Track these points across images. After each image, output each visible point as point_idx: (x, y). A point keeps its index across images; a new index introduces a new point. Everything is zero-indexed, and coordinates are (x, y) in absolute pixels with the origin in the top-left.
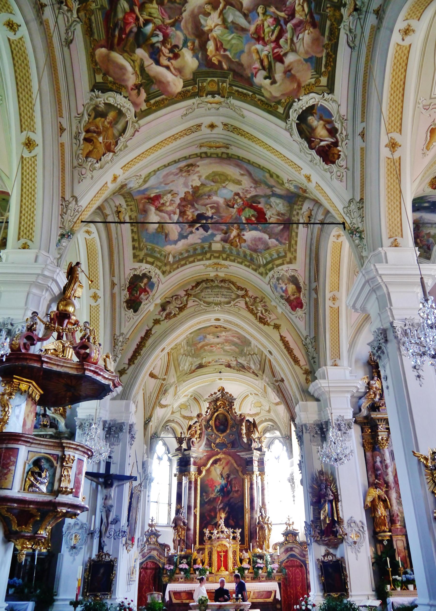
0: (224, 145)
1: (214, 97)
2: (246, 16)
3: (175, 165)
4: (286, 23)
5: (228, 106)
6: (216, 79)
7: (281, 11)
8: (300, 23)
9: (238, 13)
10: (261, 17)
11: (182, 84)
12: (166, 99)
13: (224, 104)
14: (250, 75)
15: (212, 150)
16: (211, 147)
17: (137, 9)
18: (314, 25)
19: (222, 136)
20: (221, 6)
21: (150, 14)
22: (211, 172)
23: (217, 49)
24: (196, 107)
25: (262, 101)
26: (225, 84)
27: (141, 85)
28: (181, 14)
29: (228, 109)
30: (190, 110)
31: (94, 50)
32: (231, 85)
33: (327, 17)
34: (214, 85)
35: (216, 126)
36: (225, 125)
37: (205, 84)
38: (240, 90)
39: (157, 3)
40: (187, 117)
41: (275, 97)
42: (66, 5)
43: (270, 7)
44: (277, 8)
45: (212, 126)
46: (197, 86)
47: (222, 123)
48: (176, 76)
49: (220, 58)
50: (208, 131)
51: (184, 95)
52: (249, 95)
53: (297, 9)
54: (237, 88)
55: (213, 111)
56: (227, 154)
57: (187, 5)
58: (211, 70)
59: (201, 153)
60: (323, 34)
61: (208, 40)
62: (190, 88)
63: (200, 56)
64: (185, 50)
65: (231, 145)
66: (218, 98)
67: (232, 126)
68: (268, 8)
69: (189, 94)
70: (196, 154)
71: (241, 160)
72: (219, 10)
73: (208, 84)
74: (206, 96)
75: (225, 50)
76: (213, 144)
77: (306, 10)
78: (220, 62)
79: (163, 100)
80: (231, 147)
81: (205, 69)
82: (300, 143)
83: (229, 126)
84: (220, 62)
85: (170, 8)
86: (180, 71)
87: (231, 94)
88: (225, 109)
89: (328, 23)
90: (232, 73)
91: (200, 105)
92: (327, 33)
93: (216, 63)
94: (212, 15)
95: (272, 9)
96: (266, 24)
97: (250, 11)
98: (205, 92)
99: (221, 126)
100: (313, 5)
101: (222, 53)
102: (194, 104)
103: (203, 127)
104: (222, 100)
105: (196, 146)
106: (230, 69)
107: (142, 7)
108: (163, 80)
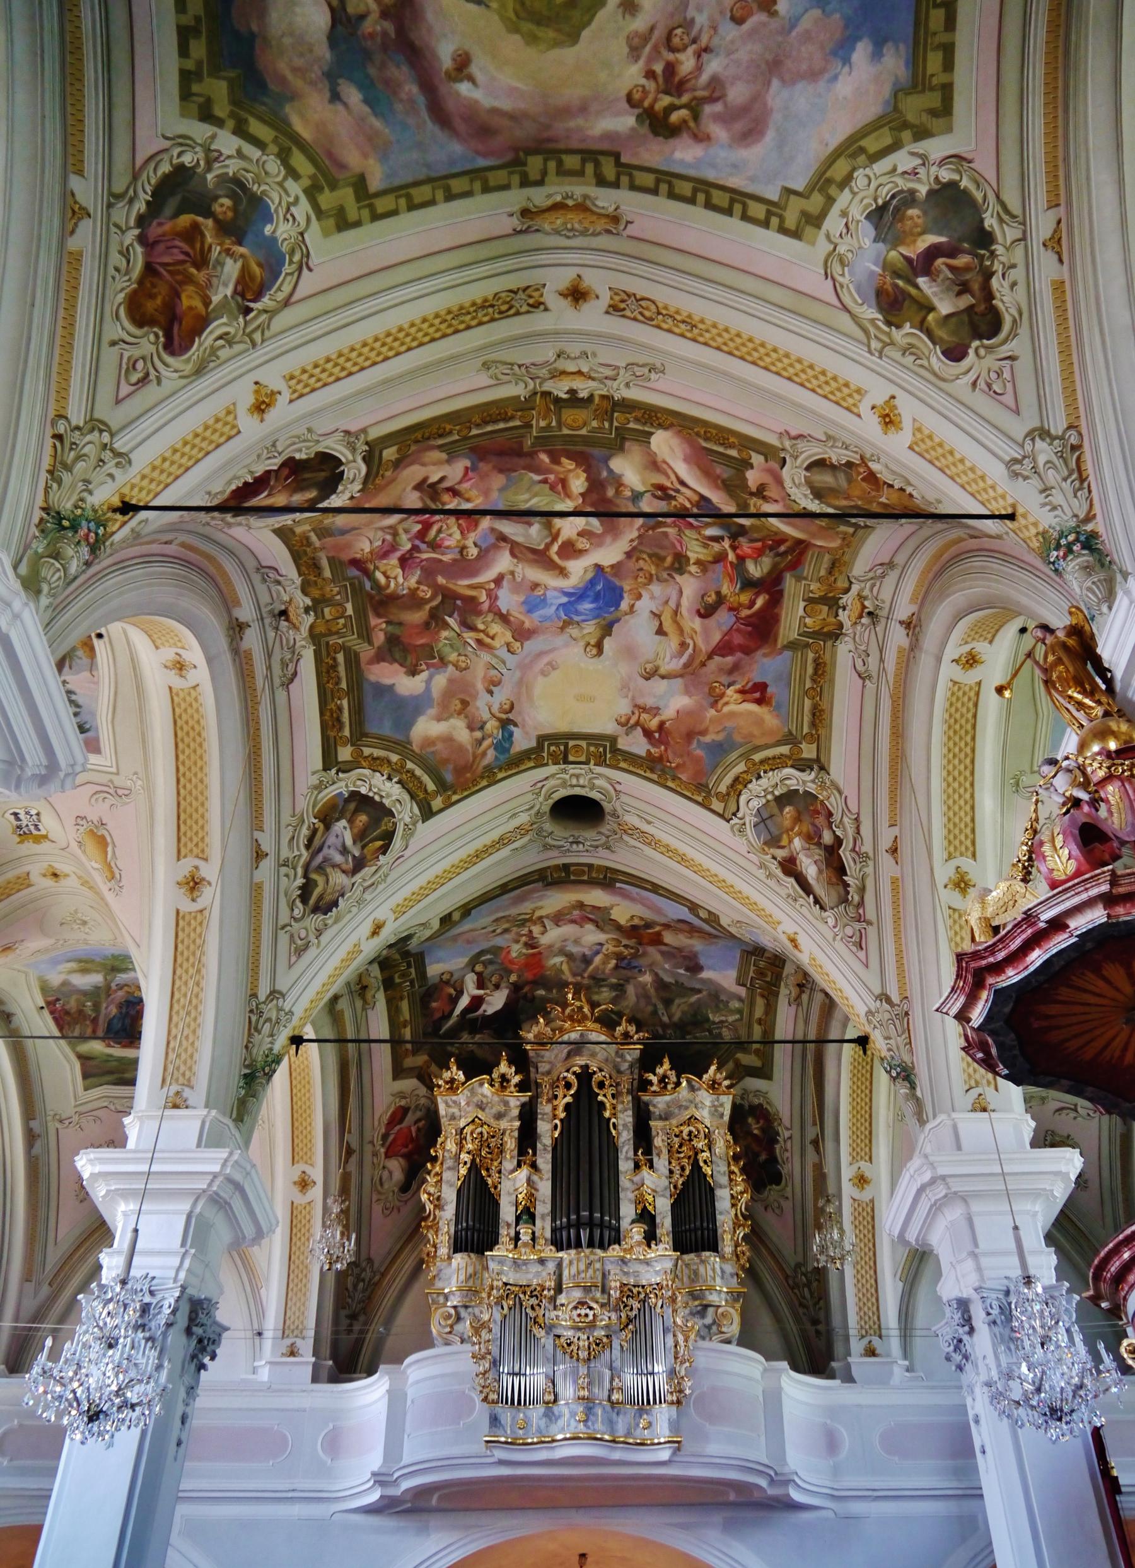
0: (537, 223)
1: (572, 392)
2: (503, 538)
3: (711, 175)
4: (415, 548)
5: (533, 370)
6: (566, 431)
7: (427, 560)
8: (385, 555)
9: (520, 539)
10: (469, 543)
11: (654, 440)
12: (698, 434)
13: (543, 373)
14: (481, 465)
15: (579, 190)
16: (582, 207)
17: (731, 556)
18: (356, 563)
19: (544, 258)
20: (555, 548)
21: (706, 546)
22: (585, 34)
23: (564, 482)
24: (622, 372)
25: (441, 436)
26: (543, 424)
27: (752, 494)
28: (640, 537)
29: (527, 361)
30: (639, 371)
31: (841, 547)
32: (528, 425)
33: (333, 581)
34: (569, 421)
35: (564, 295)
36: (537, 305)
37: (595, 424)
38: (502, 425)
39: (688, 559)
40: (650, 360)
41: (411, 464)
42: (864, 607)
43: (455, 560)
44: (440, 561)
45: (577, 294)
46: (615, 424)
47: (546, 309)
48: (665, 462)
49: (556, 468)
50: (593, 280)
51: (650, 417)
52: (478, 426)
53: (399, 571)
54: (511, 424)
55: (574, 349)
56: (525, 183)
57: (627, 548)
58: (579, 448)
59: (616, 185)
60: (331, 560)
61: (582, 495)
62: (632, 425)
63: (605, 474)
64: (641, 488)
65: (517, 232)
66: (560, 389)
67: (518, 313)
68: (458, 557)
69: (639, 414)
70: (633, 187)
71: (473, 173)
72: (560, 541)
73: (585, 424)
74: (592, 396)
75: (545, 481)
76: (575, 220)
77: (379, 576)
78: (558, 463)
79: (707, 439)
80: (515, 222)
81: (596, 452)
82: (318, 442)
83: (525, 308)
84: (555, 460)
85: (662, 547)
86: (654, 464)
87: (524, 405)
88: (539, 360)
89: (327, 573)
90: (526, 449)
91: (608, 372)
92: (325, 563)
93: (564, 460)
94: (575, 532)
95: (446, 558)
96: (457, 535)
97: (495, 547)
98: (593, 407)
99: (550, 297)
100: (368, 585)
101: (552, 477)
102: (627, 385)
103: (605, 299)
104: (548, 386)
105: (631, 230)
106: (532, 454)
107: (720, 558)
108: (698, 473)
